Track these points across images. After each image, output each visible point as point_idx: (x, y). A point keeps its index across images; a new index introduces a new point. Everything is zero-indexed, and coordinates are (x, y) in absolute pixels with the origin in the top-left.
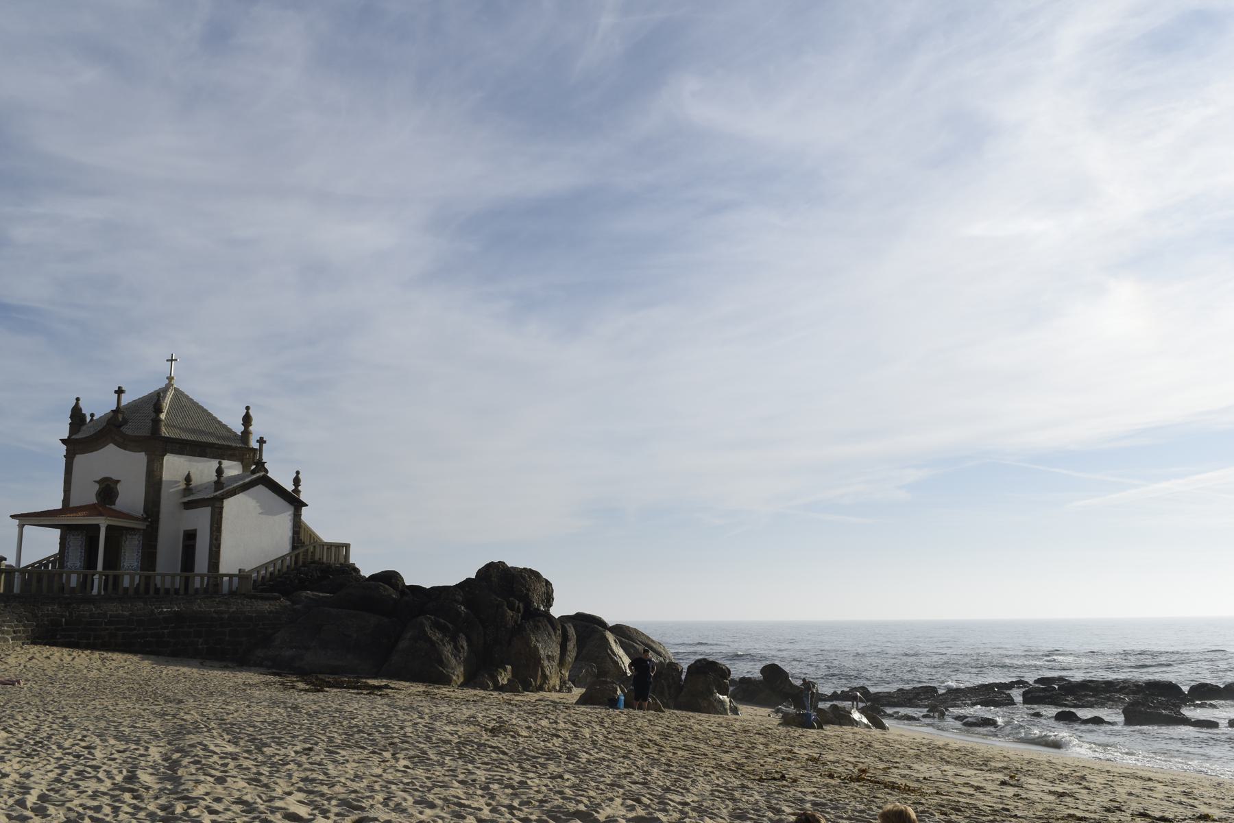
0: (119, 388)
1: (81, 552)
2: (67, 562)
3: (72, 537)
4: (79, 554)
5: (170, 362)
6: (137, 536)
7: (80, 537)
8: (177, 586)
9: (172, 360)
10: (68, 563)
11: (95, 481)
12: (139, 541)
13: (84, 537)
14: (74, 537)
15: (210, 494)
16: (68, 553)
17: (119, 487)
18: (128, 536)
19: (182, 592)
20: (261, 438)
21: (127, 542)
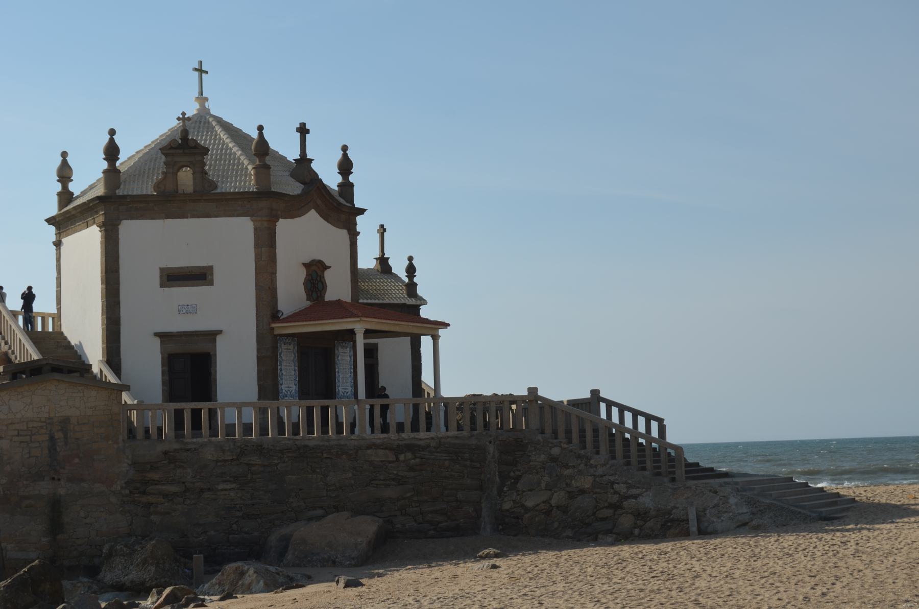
0: (304, 124)
1: (295, 371)
2: (281, 384)
3: (284, 347)
4: (293, 372)
5: (197, 74)
6: (348, 349)
7: (291, 347)
8: (400, 419)
9: (200, 71)
10: (283, 386)
11: (304, 265)
12: (350, 357)
13: (296, 348)
14: (286, 347)
15: (401, 297)
16: (281, 370)
17: (327, 274)
18: (341, 350)
19: (408, 426)
20: (382, 226)
21: (339, 358)
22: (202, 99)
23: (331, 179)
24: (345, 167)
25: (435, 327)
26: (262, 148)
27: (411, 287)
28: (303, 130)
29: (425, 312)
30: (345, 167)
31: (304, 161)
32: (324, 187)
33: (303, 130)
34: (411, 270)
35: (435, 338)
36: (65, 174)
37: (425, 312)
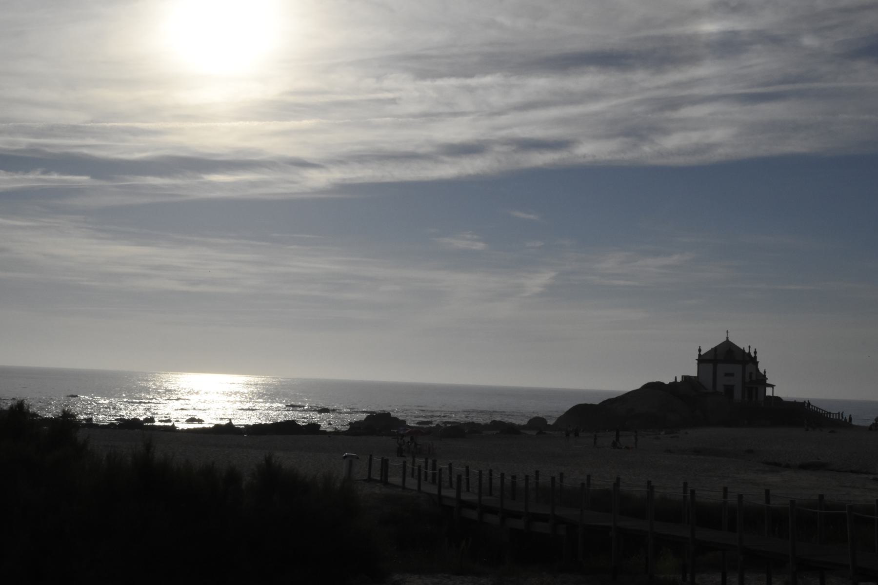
22: (727, 338)
23: (753, 355)
24: (755, 353)
25: (772, 386)
26: (744, 351)
27: (765, 376)
28: (749, 347)
29: (768, 382)
30: (755, 353)
31: (749, 353)
32: (751, 355)
33: (749, 347)
34: (765, 372)
35: (773, 388)
36: (700, 350)
37: (768, 382)
